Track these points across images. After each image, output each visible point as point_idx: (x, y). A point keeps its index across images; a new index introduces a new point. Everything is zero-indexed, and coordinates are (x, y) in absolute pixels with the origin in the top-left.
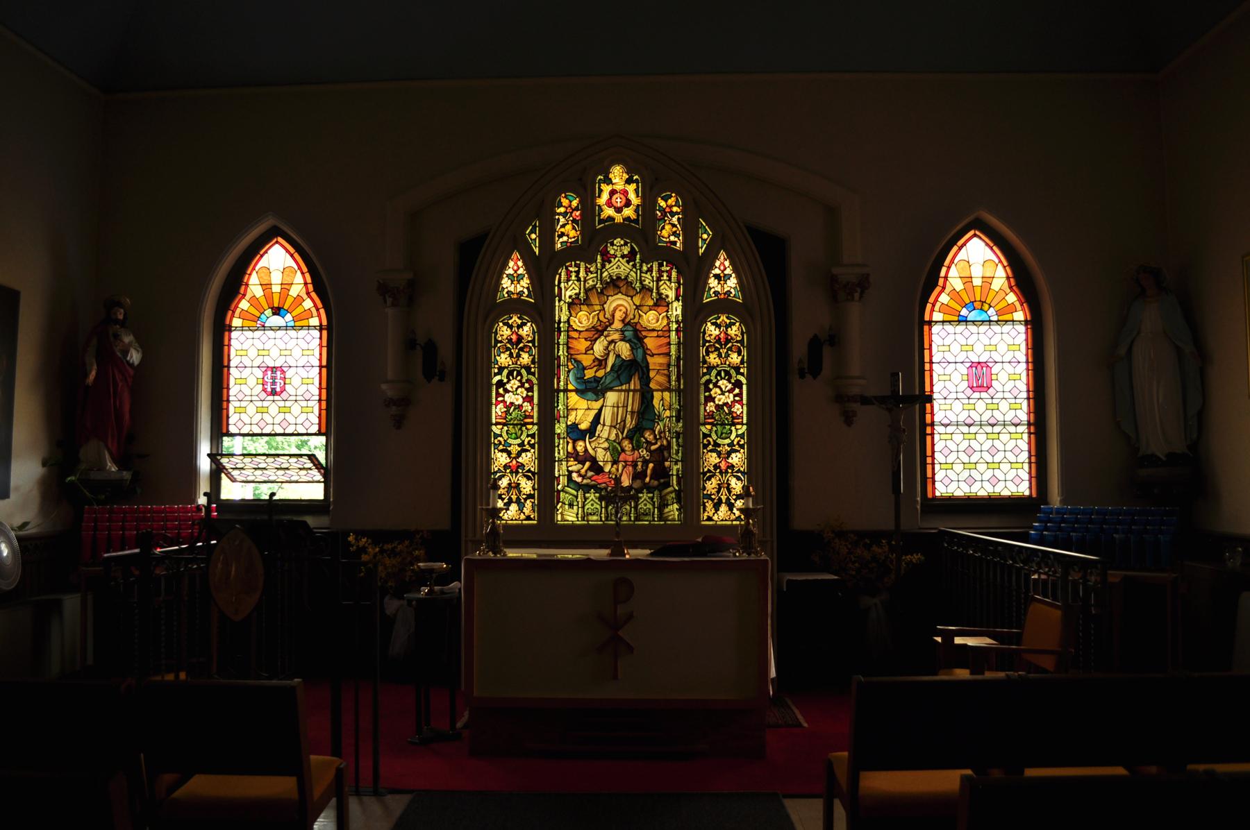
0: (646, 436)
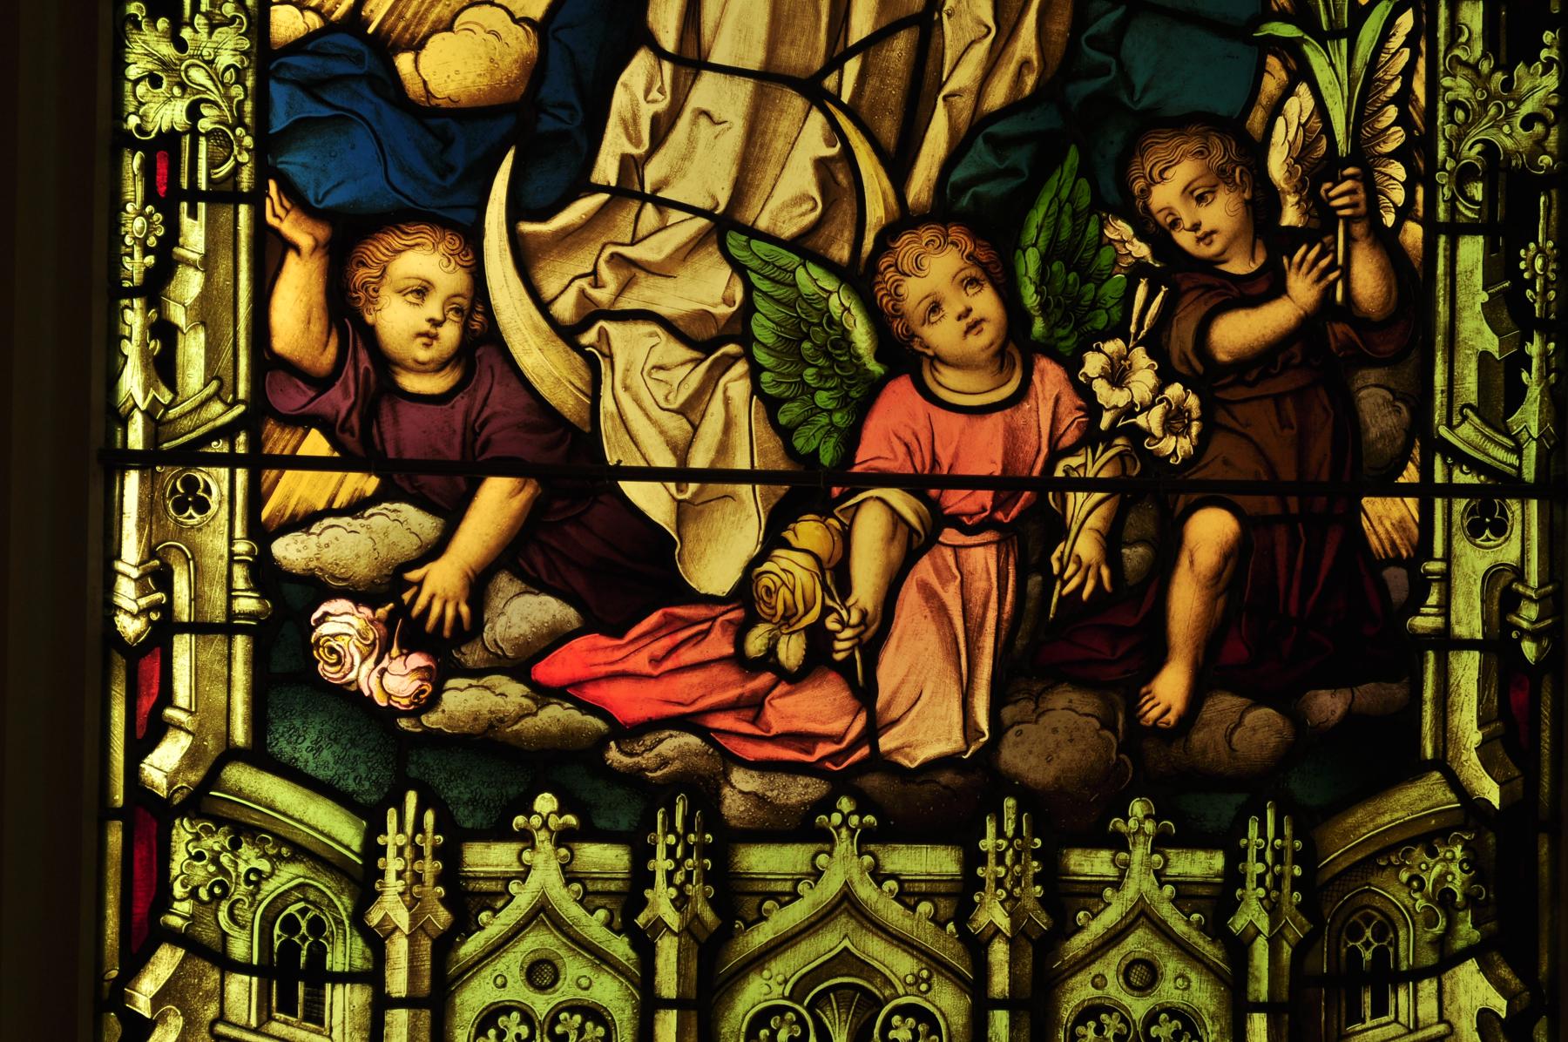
0: (1165, 196)
